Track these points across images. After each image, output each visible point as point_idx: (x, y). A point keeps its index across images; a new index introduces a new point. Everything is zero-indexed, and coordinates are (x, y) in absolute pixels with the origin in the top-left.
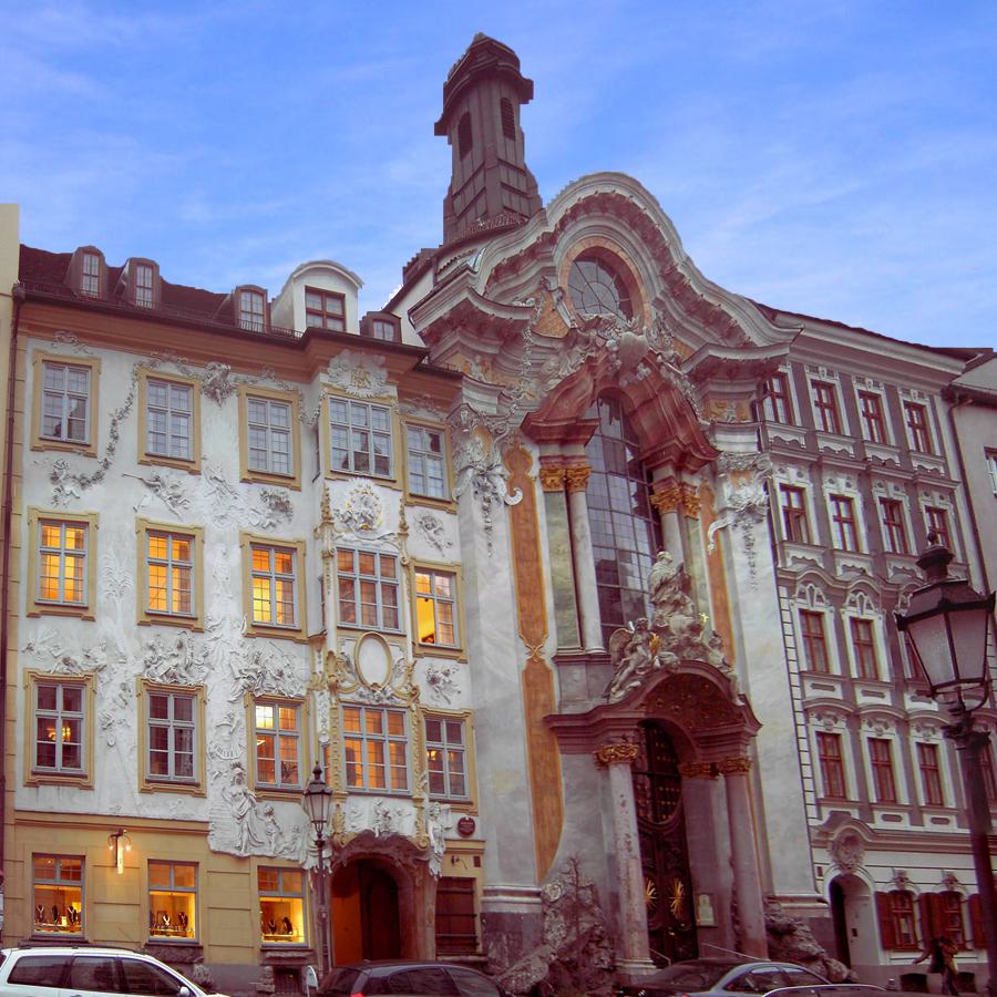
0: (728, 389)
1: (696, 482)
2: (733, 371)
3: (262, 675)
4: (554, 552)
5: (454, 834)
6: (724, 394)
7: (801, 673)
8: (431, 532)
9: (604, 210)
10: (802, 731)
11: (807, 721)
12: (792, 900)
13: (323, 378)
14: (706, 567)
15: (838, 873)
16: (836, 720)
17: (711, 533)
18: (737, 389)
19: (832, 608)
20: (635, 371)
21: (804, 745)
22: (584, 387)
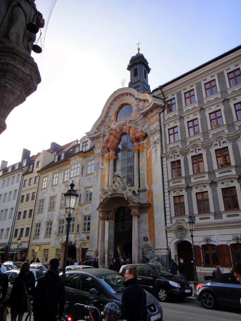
0: (152, 115)
1: (145, 141)
2: (151, 110)
3: (60, 216)
4: (106, 176)
5: (86, 239)
6: (152, 116)
7: (168, 182)
8: (89, 181)
9: (119, 98)
10: (167, 198)
11: (169, 194)
12: (160, 249)
13: (71, 163)
14: (145, 162)
15: (177, 240)
16: (181, 191)
17: (148, 152)
18: (154, 113)
19: (183, 157)
20: (123, 128)
21: (167, 202)
22: (111, 139)
